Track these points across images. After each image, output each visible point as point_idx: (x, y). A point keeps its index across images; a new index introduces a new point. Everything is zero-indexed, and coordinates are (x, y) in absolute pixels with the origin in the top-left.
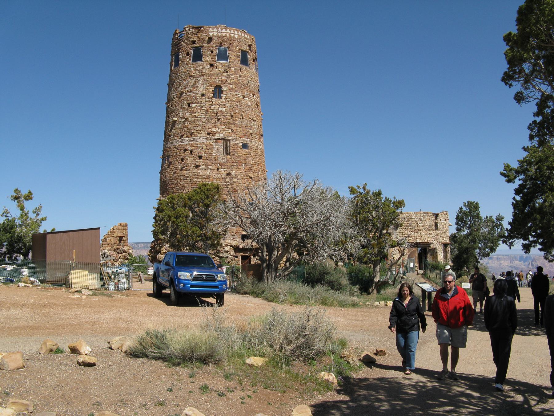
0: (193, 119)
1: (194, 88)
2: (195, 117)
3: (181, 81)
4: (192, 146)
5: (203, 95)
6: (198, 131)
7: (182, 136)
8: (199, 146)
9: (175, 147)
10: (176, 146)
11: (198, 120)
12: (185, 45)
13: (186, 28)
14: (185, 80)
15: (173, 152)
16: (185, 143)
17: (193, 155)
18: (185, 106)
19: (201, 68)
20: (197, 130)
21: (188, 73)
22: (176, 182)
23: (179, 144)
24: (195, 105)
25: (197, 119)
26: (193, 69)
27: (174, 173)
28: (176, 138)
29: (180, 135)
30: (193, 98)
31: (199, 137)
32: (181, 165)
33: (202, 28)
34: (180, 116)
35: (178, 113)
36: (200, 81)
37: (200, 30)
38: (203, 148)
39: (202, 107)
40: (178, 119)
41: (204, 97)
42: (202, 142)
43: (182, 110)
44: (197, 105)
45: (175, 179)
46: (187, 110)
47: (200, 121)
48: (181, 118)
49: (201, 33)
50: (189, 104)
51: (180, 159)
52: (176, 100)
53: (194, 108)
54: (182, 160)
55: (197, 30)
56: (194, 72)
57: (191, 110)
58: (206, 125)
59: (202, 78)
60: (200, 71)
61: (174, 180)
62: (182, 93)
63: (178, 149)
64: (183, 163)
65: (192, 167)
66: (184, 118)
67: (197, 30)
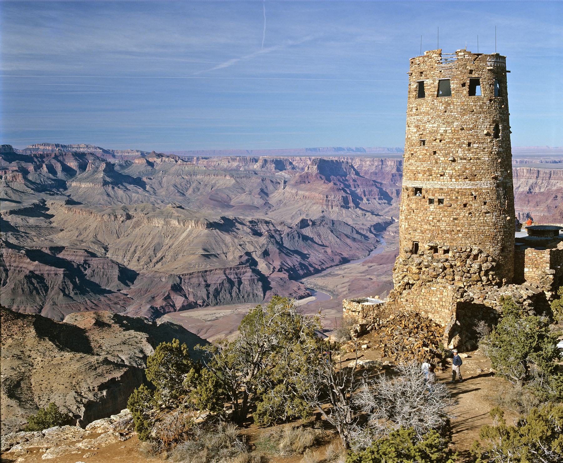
2: (479, 159)
4: (476, 191)
10: (456, 190)
12: (459, 72)
13: (459, 52)
19: (481, 103)
21: (466, 107)
22: (458, 229)
24: (477, 145)
28: (454, 180)
32: (464, 211)
37: (477, 58)
39: (484, 148)
42: (487, 187)
43: (460, 150)
47: (483, 163)
50: (469, 144)
57: (472, 150)
59: (483, 115)
60: (481, 107)
61: (454, 227)
63: (458, 192)
64: (466, 208)
65: (477, 215)
66: (465, 159)
67: (474, 58)
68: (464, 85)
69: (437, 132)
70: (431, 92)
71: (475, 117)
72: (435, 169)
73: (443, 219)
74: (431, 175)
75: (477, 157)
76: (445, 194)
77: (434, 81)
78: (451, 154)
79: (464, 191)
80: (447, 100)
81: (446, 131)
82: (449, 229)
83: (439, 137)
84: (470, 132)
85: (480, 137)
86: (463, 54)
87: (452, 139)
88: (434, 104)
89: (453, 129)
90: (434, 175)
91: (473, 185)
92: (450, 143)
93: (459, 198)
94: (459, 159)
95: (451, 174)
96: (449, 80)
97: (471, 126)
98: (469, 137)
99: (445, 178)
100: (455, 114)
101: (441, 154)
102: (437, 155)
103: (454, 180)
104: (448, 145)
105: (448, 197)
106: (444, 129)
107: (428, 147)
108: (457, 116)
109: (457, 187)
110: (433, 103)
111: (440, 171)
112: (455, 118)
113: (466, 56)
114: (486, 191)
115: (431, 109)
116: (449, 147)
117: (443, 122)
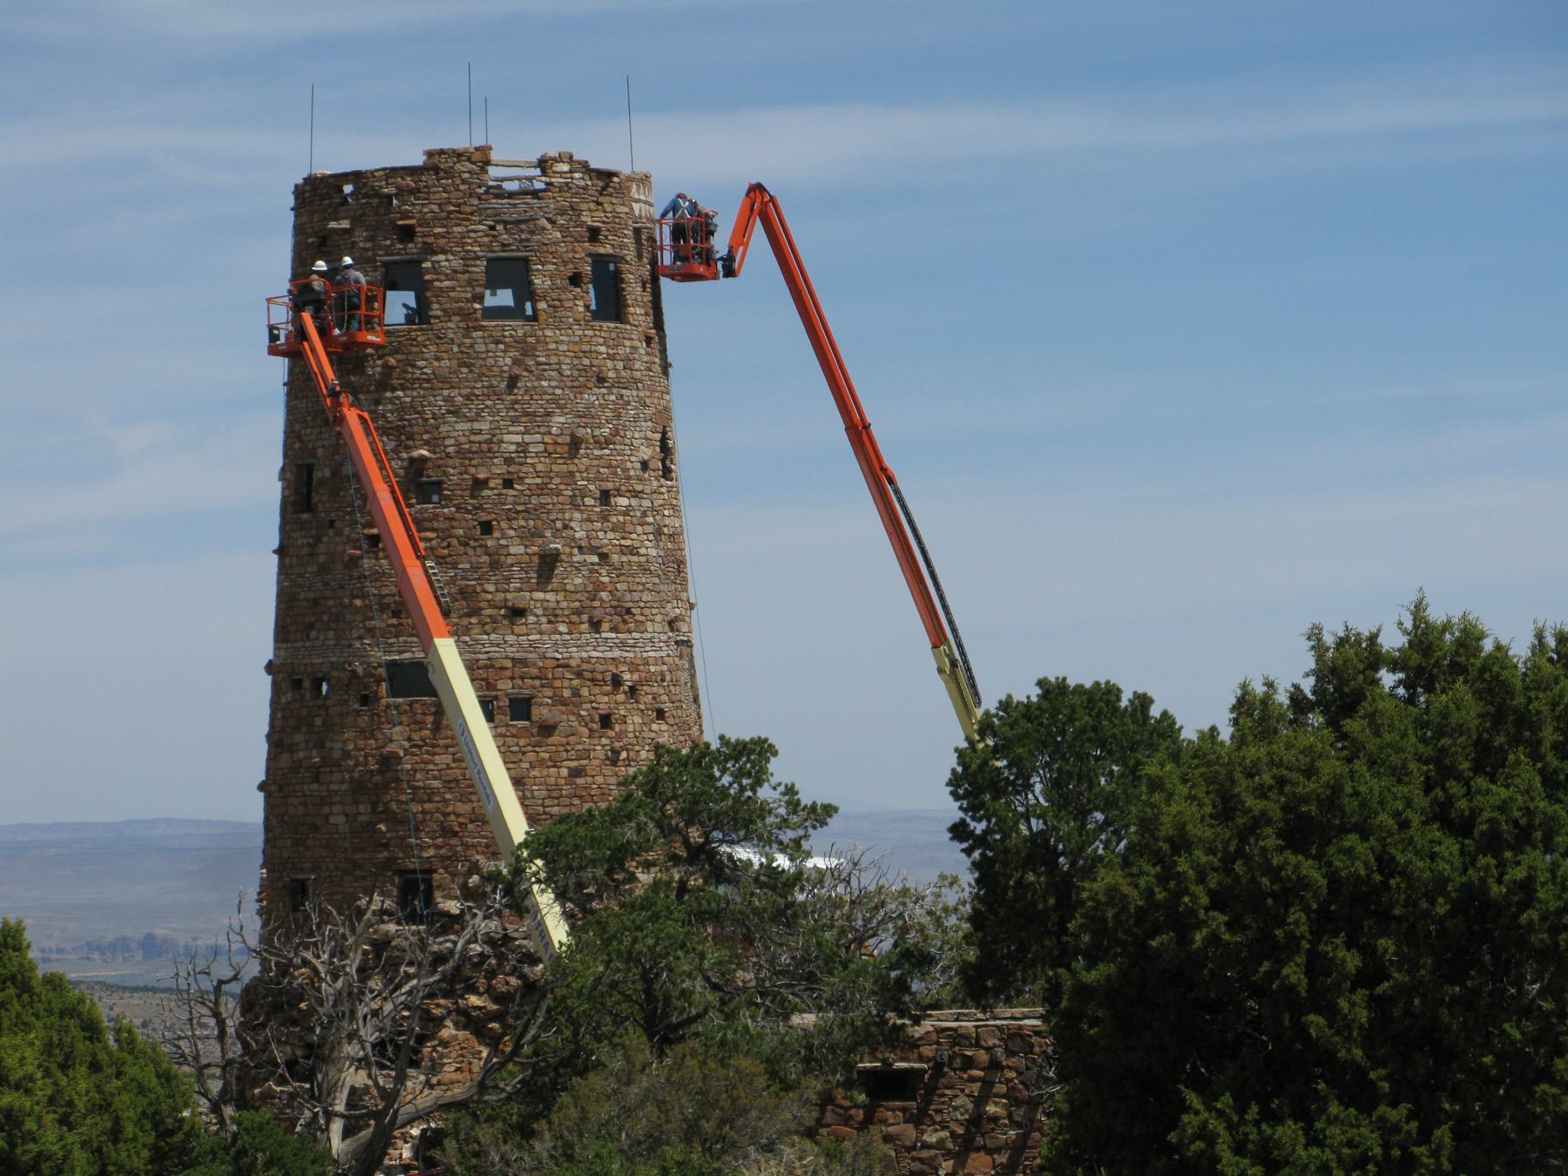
0: (624, 559)
1: (616, 432)
3: (558, 391)
4: (633, 667)
5: (645, 465)
6: (647, 611)
7: (596, 626)
8: (653, 669)
9: (567, 666)
10: (573, 663)
11: (639, 564)
13: (555, 160)
14: (580, 389)
15: (557, 683)
16: (609, 655)
17: (642, 707)
18: (592, 502)
19: (628, 350)
20: (642, 604)
21: (587, 362)
23: (585, 655)
25: (635, 559)
26: (603, 349)
27: (576, 773)
29: (585, 617)
30: (615, 473)
31: (649, 635)
33: (616, 179)
34: (573, 539)
35: (566, 527)
36: (628, 403)
38: (663, 680)
39: (644, 514)
40: (567, 550)
41: (646, 476)
42: (658, 654)
43: (577, 515)
44: (634, 502)
45: (581, 797)
46: (604, 518)
48: (580, 548)
49: (614, 201)
51: (597, 719)
52: (540, 467)
53: (625, 514)
54: (606, 721)
55: (601, 184)
56: (610, 364)
57: (614, 519)
58: (662, 587)
59: (635, 393)
62: (575, 444)
63: (579, 675)
64: (611, 733)
66: (593, 550)
67: (601, 184)
68: (575, 280)
69: (489, 449)
70: (458, 300)
71: (613, 397)
72: (491, 588)
73: (535, 773)
74: (475, 612)
75: (628, 543)
76: (537, 683)
77: (468, 259)
78: (548, 534)
79: (600, 668)
80: (520, 332)
81: (523, 448)
82: (555, 810)
83: (500, 469)
84: (607, 452)
85: (632, 473)
86: (566, 168)
87: (548, 475)
88: (472, 346)
89: (547, 439)
90: (489, 612)
91: (623, 645)
92: (542, 489)
93: (585, 692)
94: (576, 551)
95: (553, 605)
96: (526, 261)
97: (606, 431)
98: (602, 470)
99: (531, 619)
100: (554, 383)
101: (512, 533)
102: (497, 534)
103: (563, 628)
104: (534, 500)
105: (549, 692)
106: (518, 438)
107: (455, 506)
108: (558, 391)
109: (576, 655)
110: (468, 341)
111: (509, 596)
112: (555, 401)
113: (577, 175)
114: (658, 668)
115: (460, 365)
116: (543, 505)
117: (512, 413)
